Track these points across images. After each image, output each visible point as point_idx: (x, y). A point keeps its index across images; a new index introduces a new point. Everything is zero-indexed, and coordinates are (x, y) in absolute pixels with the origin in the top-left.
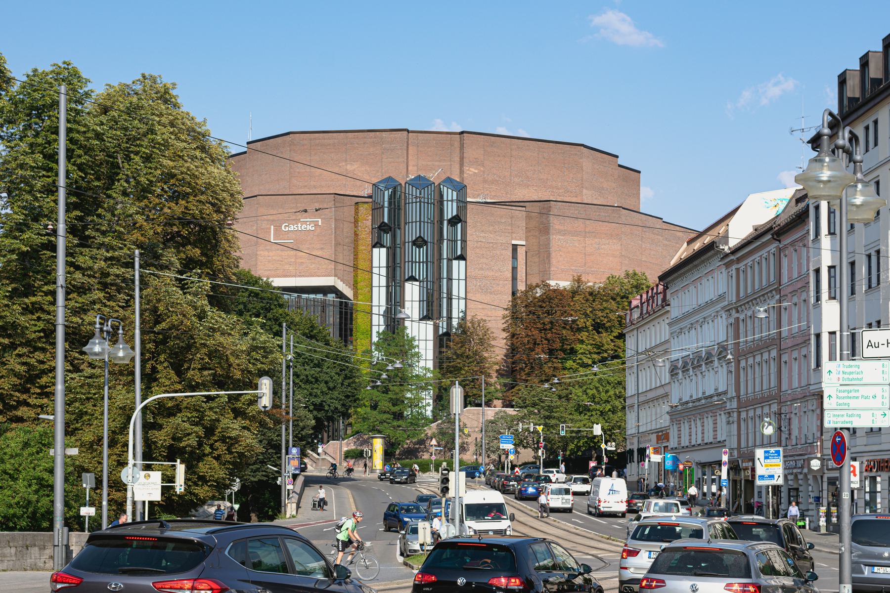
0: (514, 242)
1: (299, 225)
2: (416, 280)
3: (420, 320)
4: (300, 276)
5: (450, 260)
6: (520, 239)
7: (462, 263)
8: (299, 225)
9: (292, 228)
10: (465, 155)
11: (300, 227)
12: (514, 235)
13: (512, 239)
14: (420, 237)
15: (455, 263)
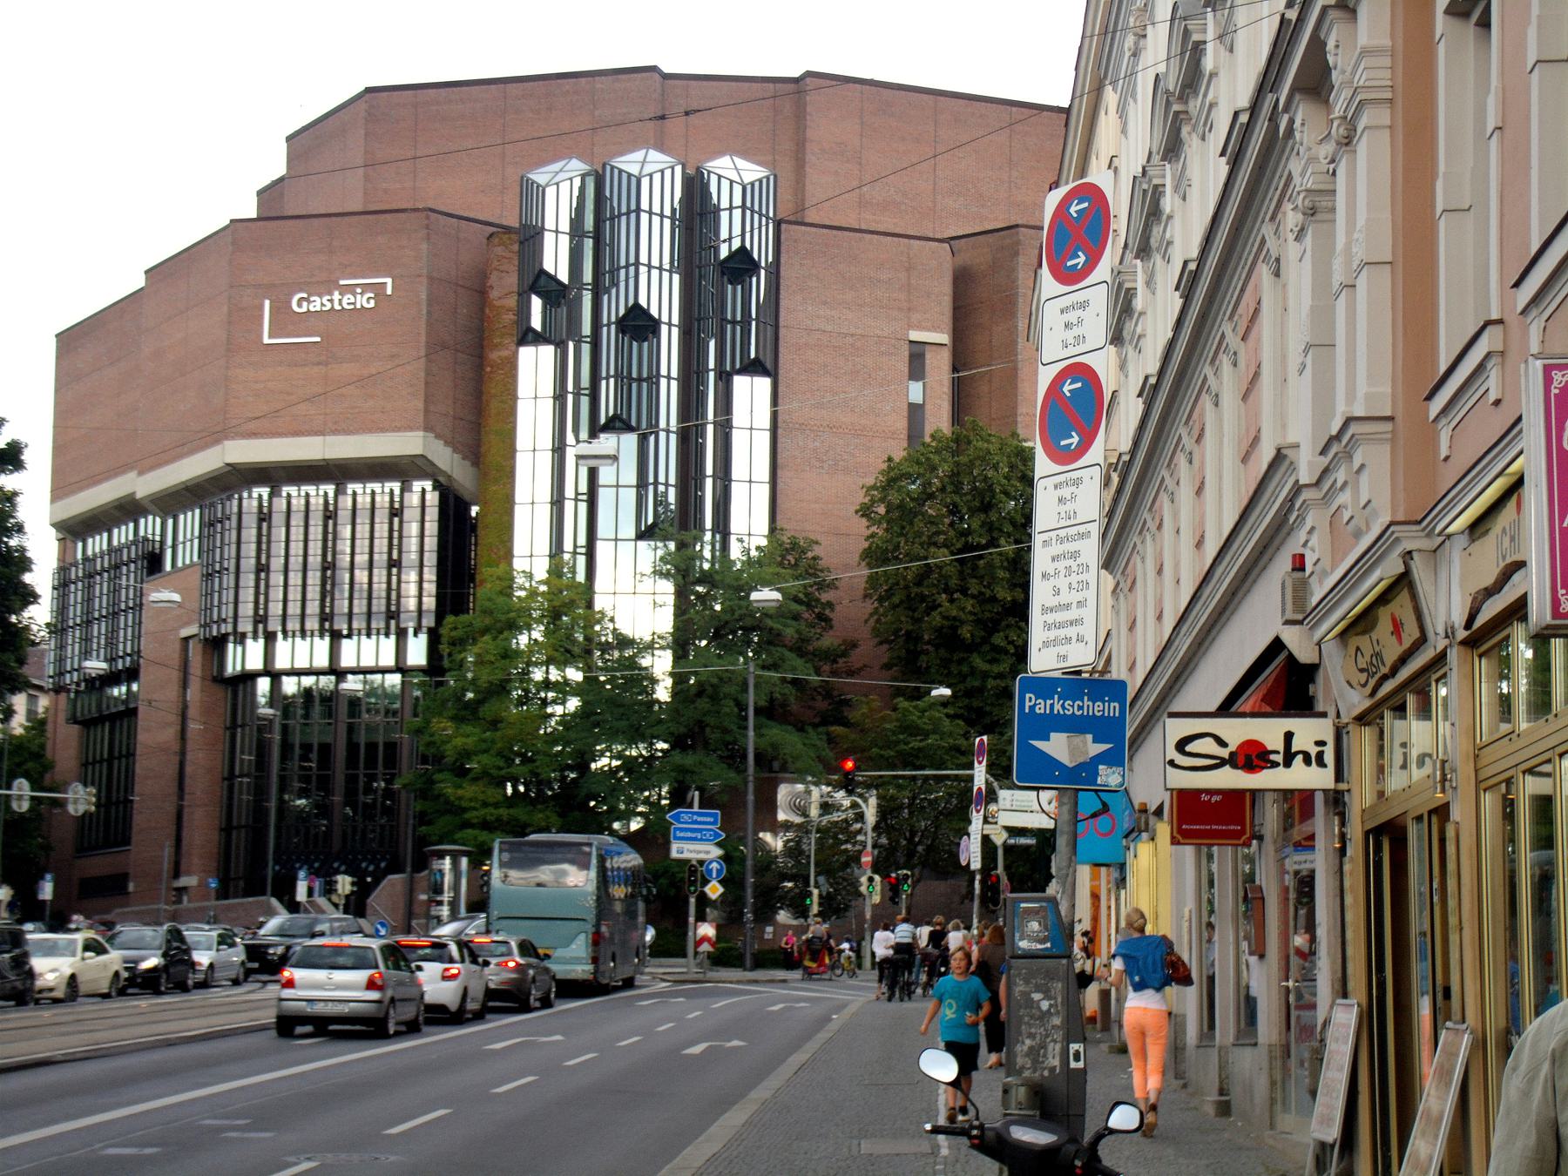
0: (915, 335)
1: (336, 296)
2: (630, 429)
3: (641, 536)
4: (335, 432)
5: (725, 379)
6: (934, 328)
7: (763, 384)
8: (336, 296)
9: (316, 304)
10: (809, 133)
11: (339, 301)
12: (915, 317)
13: (910, 327)
14: (637, 305)
15: (741, 383)
